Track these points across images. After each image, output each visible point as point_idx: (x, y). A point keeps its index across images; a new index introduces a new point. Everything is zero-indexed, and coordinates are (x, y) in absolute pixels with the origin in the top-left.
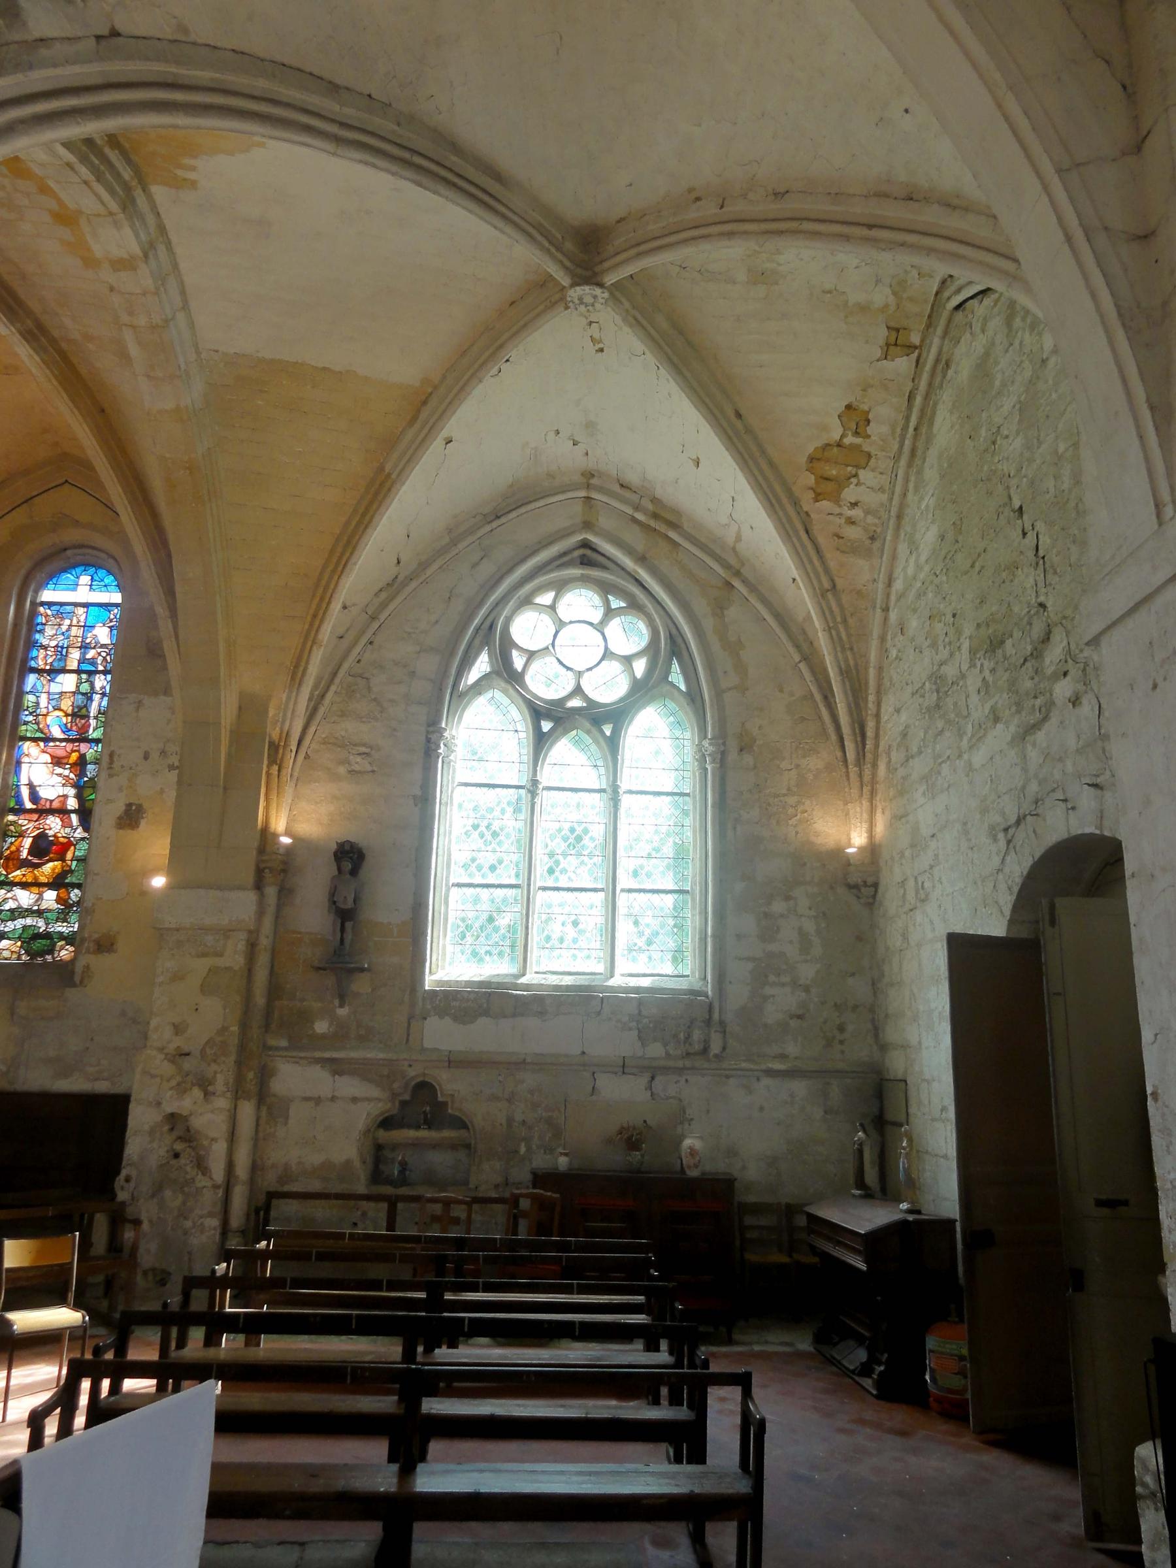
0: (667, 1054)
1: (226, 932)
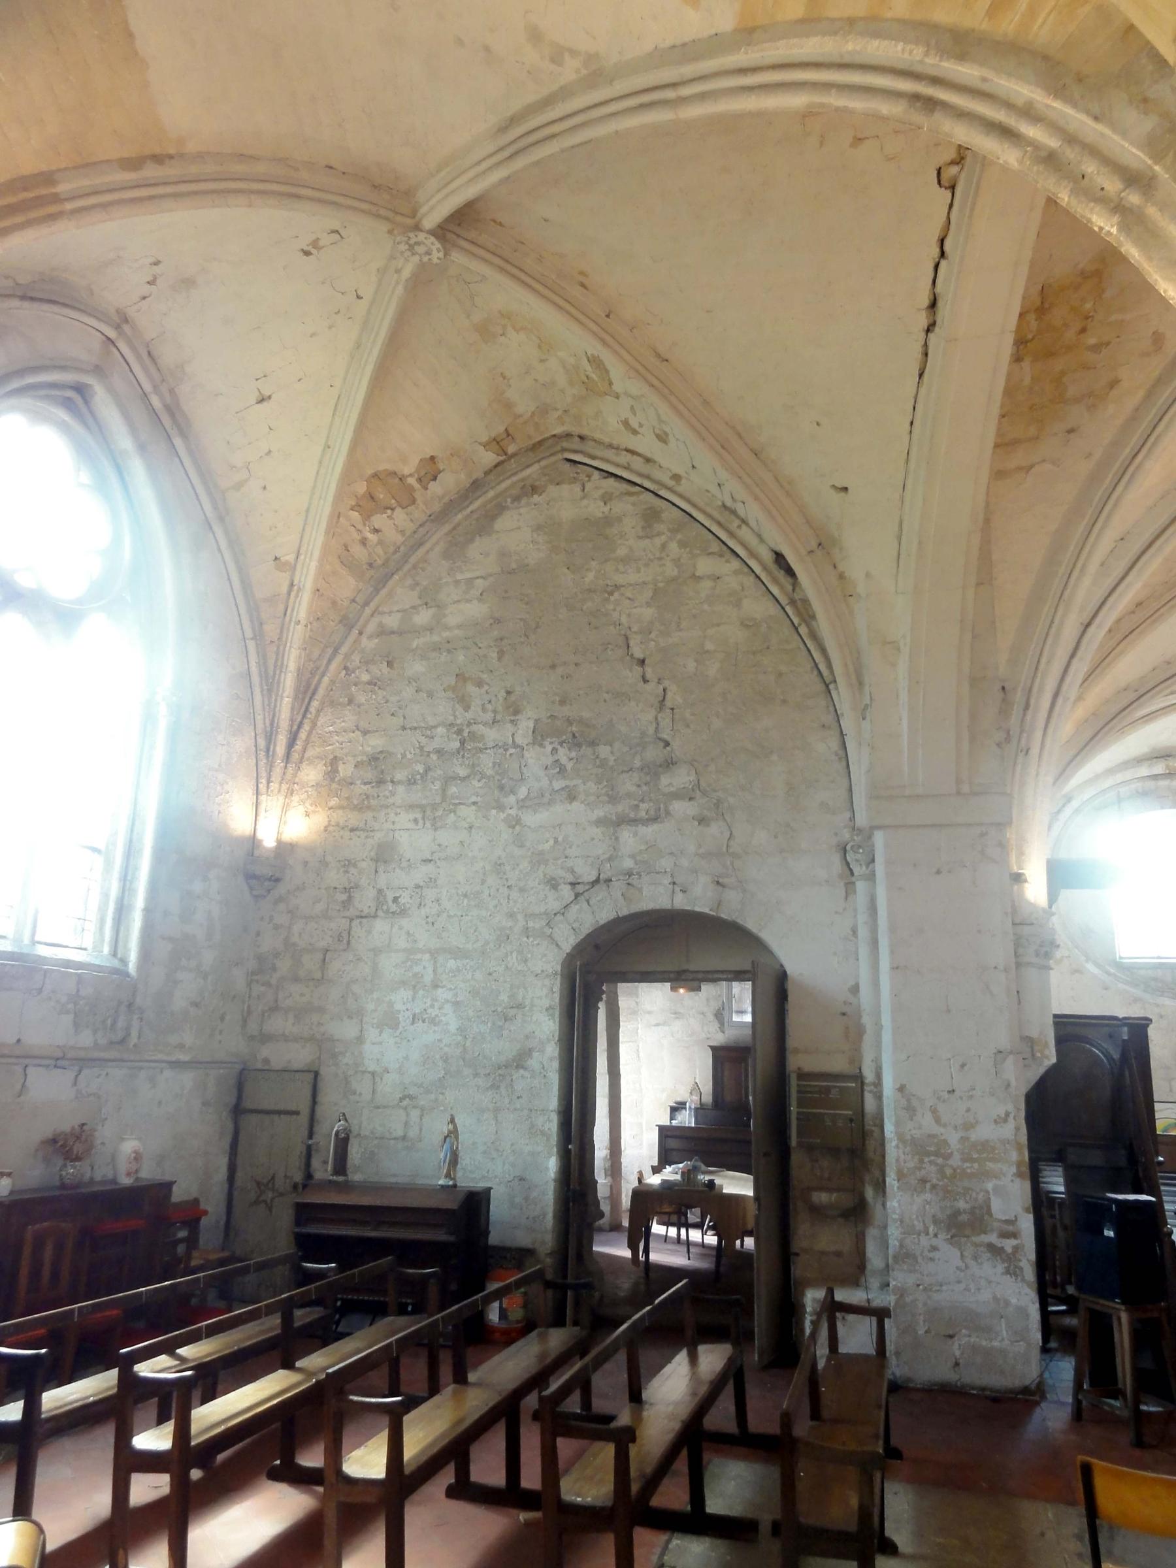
0: (96, 1044)
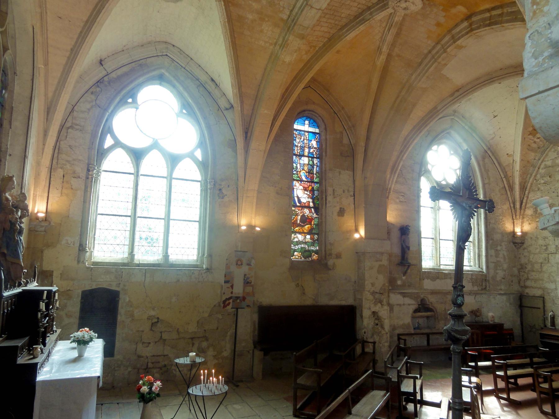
1: (382, 254)
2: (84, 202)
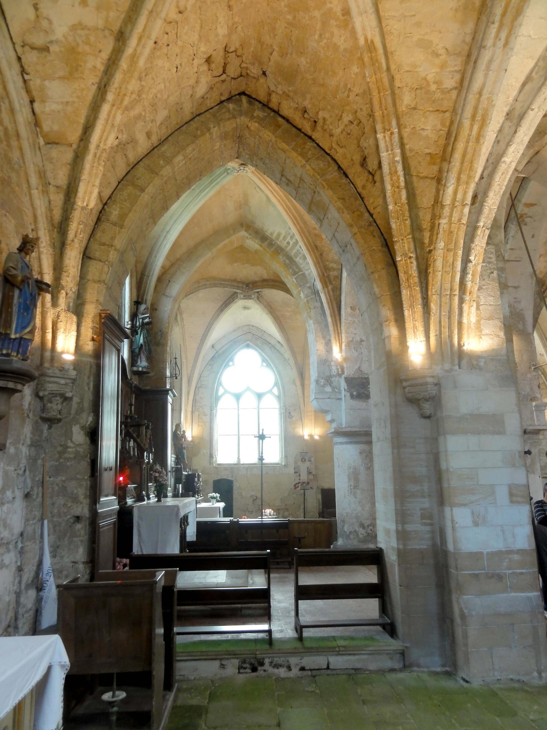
2: (211, 429)
